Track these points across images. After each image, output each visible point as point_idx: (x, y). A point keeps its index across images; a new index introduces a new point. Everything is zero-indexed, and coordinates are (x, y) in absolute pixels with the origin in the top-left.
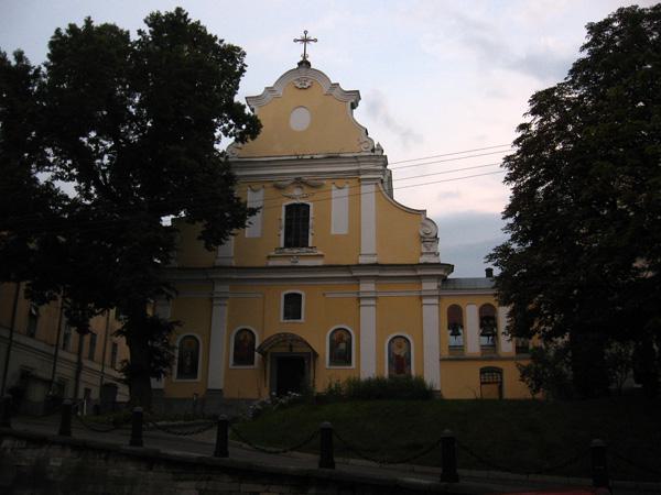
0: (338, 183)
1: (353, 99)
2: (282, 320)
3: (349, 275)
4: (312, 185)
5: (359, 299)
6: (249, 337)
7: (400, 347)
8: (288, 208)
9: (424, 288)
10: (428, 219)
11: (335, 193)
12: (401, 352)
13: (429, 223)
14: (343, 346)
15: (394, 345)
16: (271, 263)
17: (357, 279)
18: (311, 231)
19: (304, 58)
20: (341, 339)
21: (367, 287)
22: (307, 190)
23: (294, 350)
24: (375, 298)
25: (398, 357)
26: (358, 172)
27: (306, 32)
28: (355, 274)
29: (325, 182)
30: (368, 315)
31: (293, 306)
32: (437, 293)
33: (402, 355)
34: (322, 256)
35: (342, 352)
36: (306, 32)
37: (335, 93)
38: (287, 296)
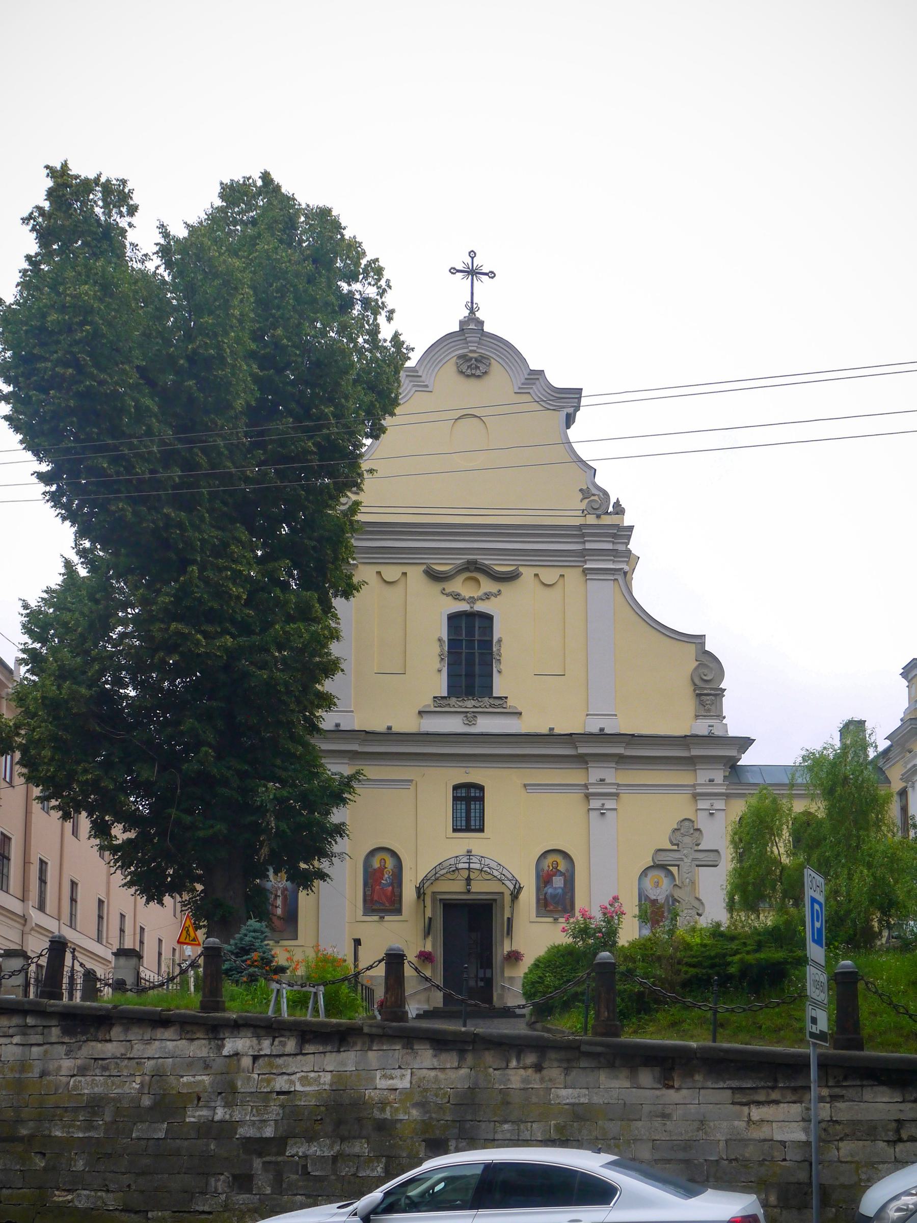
1: (568, 402)
2: (450, 833)
8: (453, 618)
14: (558, 882)
19: (472, 311)
20: (556, 872)
22: (487, 586)
23: (476, 887)
24: (617, 795)
25: (654, 902)
27: (472, 254)
28: (581, 750)
31: (469, 806)
32: (722, 790)
36: (472, 254)
37: (535, 389)
38: (456, 788)
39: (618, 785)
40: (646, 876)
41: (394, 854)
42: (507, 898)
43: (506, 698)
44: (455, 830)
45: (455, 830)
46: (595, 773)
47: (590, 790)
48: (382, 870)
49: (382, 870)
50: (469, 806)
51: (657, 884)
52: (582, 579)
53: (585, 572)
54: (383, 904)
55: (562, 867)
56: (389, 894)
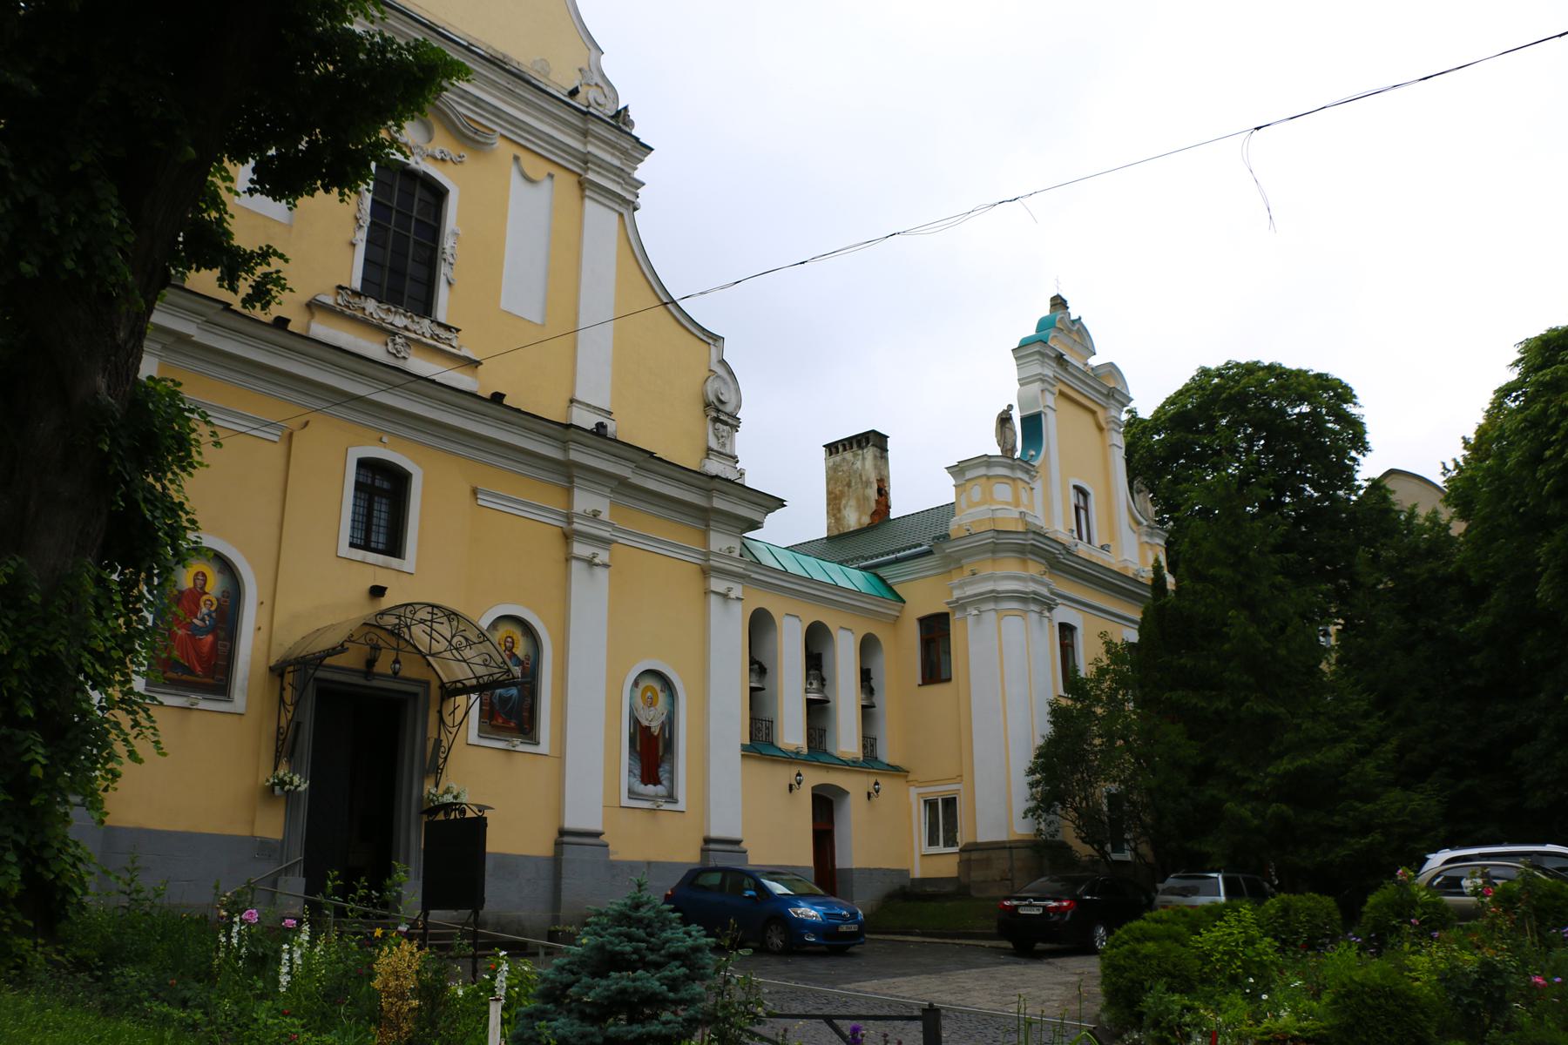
0: (527, 160)
2: (345, 550)
3: (556, 454)
5: (568, 537)
6: (215, 584)
10: (723, 362)
12: (653, 719)
13: (721, 371)
16: (323, 329)
18: (444, 270)
26: (586, 160)
30: (591, 596)
31: (382, 502)
33: (655, 727)
34: (477, 363)
35: (513, 708)
41: (226, 566)
42: (435, 692)
43: (458, 330)
44: (352, 545)
45: (352, 545)
46: (584, 501)
47: (575, 526)
48: (197, 593)
49: (197, 593)
50: (382, 502)
52: (575, 190)
53: (583, 184)
54: (191, 672)
55: (521, 649)
56: (206, 649)
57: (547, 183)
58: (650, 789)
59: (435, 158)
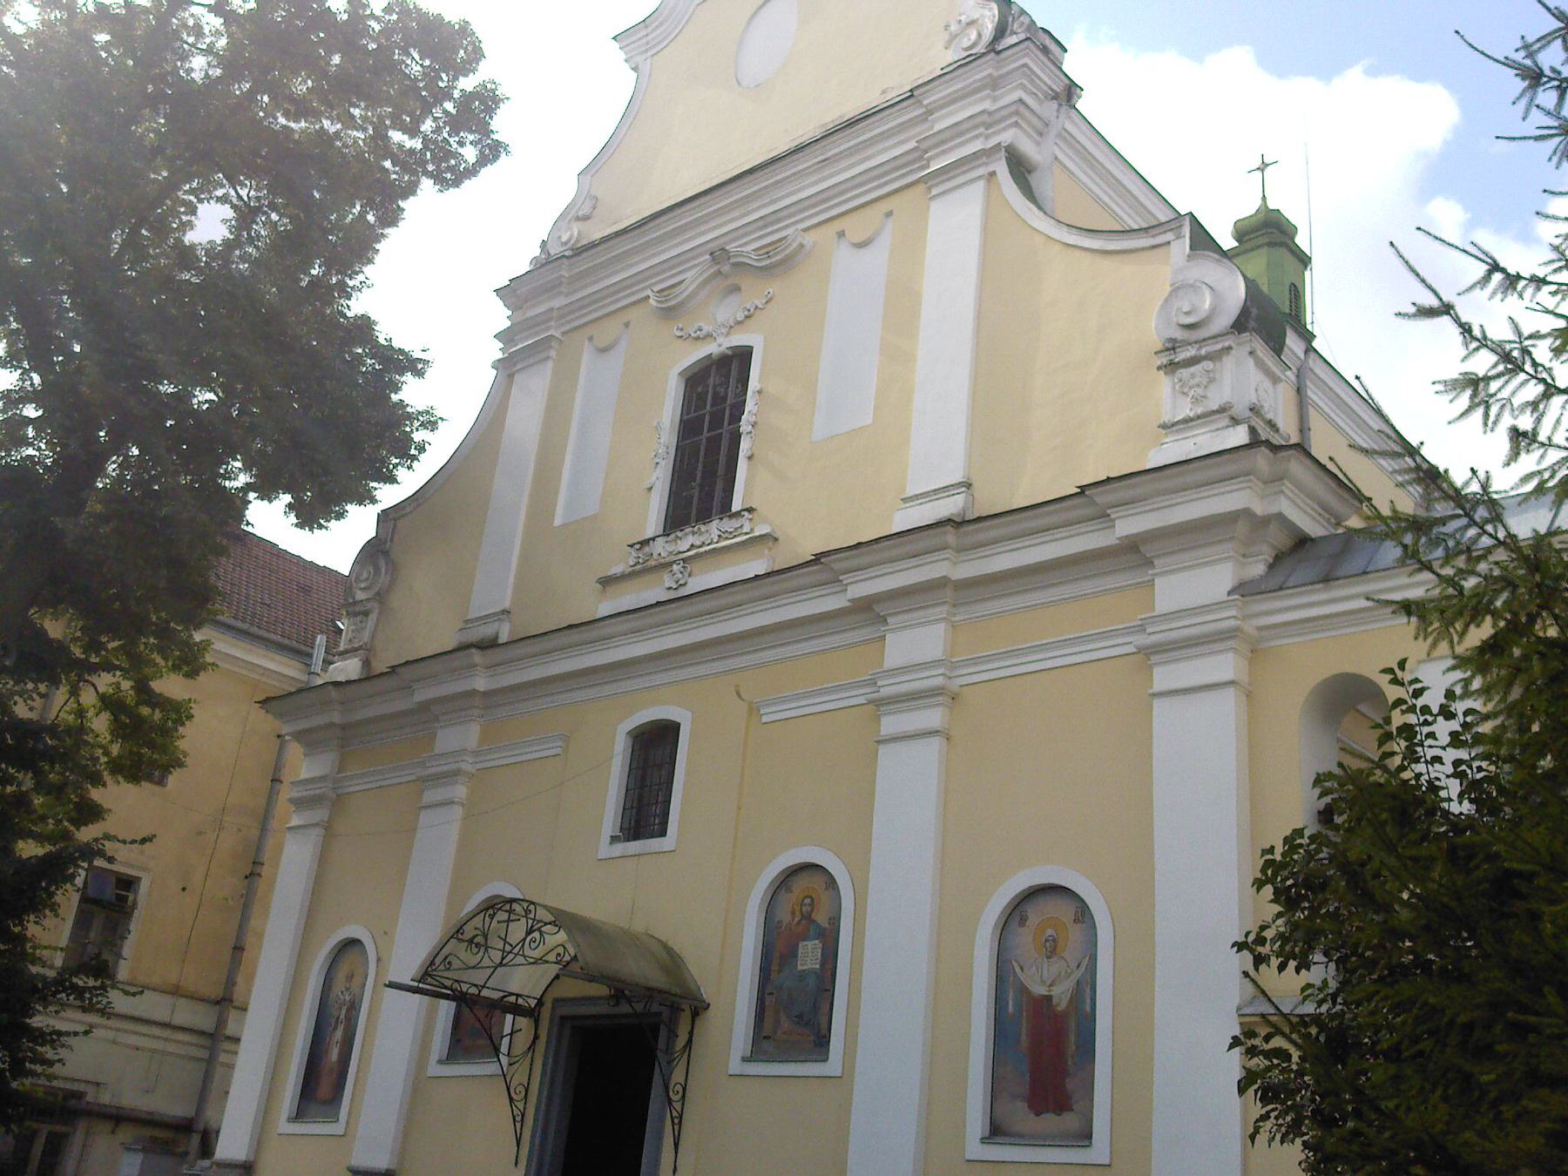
4: (778, 263)
7: (1052, 949)
9: (1163, 604)
11: (844, 260)
14: (809, 955)
15: (1025, 940)
17: (869, 611)
21: (916, 643)
29: (809, 239)
32: (1227, 618)
33: (1061, 994)
39: (954, 666)
40: (1023, 921)
43: (750, 510)
51: (1052, 949)
57: (890, 225)
58: (1050, 1121)
59: (739, 323)
